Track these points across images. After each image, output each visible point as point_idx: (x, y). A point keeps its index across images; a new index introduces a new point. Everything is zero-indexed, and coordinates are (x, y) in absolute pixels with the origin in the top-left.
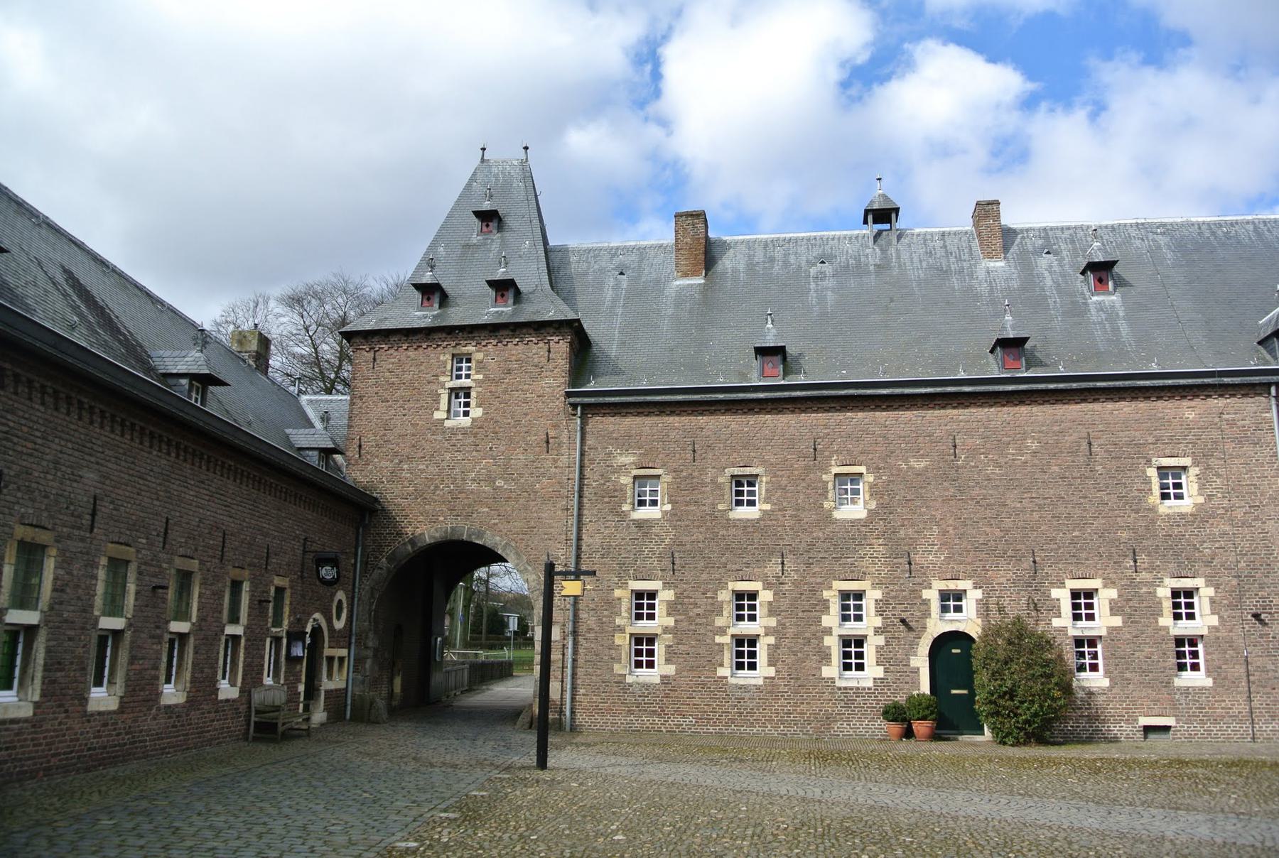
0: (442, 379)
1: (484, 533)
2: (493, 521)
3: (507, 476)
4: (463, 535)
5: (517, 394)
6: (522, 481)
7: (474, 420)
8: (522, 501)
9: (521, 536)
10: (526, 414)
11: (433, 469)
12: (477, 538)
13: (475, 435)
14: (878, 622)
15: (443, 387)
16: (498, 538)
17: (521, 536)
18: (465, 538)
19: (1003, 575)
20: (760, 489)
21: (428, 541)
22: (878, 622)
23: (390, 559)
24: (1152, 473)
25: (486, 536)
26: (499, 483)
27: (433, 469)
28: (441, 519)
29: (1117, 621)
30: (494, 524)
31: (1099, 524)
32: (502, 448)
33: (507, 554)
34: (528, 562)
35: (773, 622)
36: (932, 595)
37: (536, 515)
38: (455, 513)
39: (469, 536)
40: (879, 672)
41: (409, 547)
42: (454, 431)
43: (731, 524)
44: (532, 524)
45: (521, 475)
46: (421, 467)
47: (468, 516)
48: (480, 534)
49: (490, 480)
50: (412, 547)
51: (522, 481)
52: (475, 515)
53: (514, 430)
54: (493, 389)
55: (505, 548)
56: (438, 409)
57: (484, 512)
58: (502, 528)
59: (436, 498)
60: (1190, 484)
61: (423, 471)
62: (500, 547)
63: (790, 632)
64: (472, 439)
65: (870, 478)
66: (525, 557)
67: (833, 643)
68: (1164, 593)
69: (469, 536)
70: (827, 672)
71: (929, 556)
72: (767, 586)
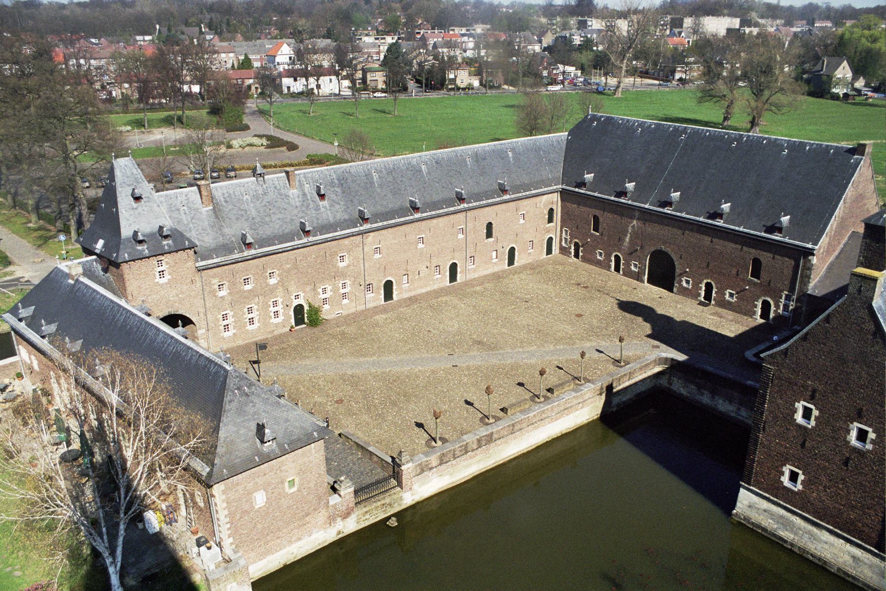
14: (282, 306)
19: (308, 288)
20: (251, 281)
22: (282, 306)
24: (339, 258)
29: (332, 293)
31: (327, 272)
35: (258, 313)
36: (293, 297)
40: (283, 318)
43: (244, 292)
60: (346, 259)
63: (262, 314)
65: (277, 272)
67: (272, 314)
68: (341, 285)
70: (271, 321)
71: (292, 288)
72: (256, 304)
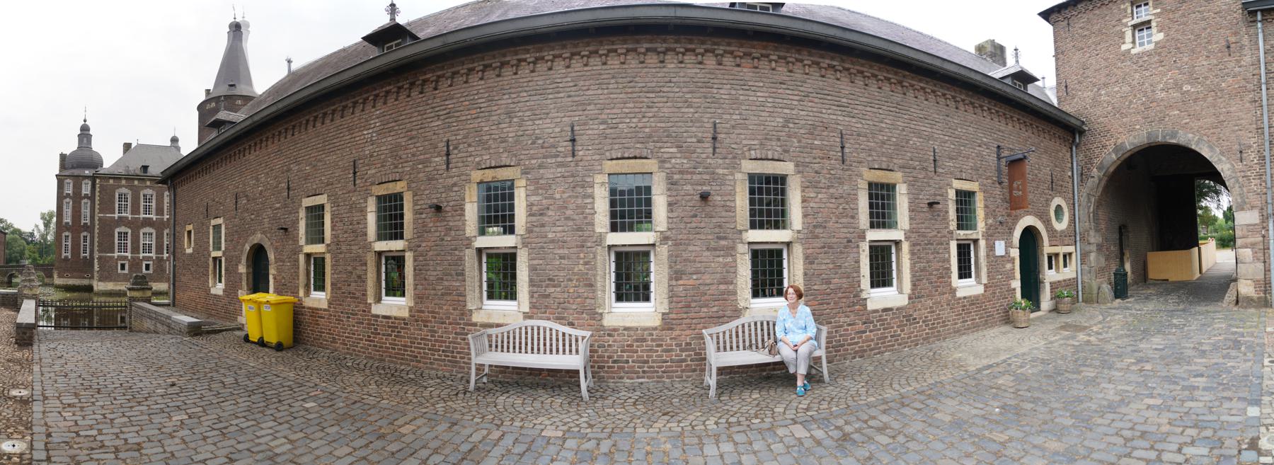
0: (1124, 21)
1: (1177, 132)
2: (1185, 121)
3: (1193, 80)
4: (1157, 137)
5: (1194, 16)
6: (1208, 82)
7: (1157, 43)
8: (1210, 99)
9: (1212, 131)
10: (1205, 29)
11: (1126, 88)
12: (1172, 137)
13: (1159, 54)
15: (1126, 26)
16: (1190, 136)
17: (1212, 131)
18: (1160, 139)
21: (1129, 148)
23: (1099, 169)
25: (1179, 135)
26: (1186, 88)
27: (1126, 88)
28: (1138, 127)
30: (1186, 124)
32: (1186, 59)
33: (1200, 148)
34: (1222, 153)
37: (1224, 110)
38: (1149, 120)
39: (1164, 137)
41: (1114, 156)
42: (1140, 56)
44: (1222, 118)
45: (1206, 78)
46: (1117, 89)
47: (1161, 120)
48: (1174, 135)
49: (1177, 86)
50: (1116, 155)
51: (1208, 82)
52: (1167, 119)
53: (1195, 43)
54: (1171, 16)
55: (1197, 143)
56: (1124, 43)
57: (1174, 115)
58: (1193, 125)
59: (1131, 111)
61: (1117, 92)
62: (1193, 143)
64: (1157, 58)
66: (1218, 150)
69: (1164, 137)
